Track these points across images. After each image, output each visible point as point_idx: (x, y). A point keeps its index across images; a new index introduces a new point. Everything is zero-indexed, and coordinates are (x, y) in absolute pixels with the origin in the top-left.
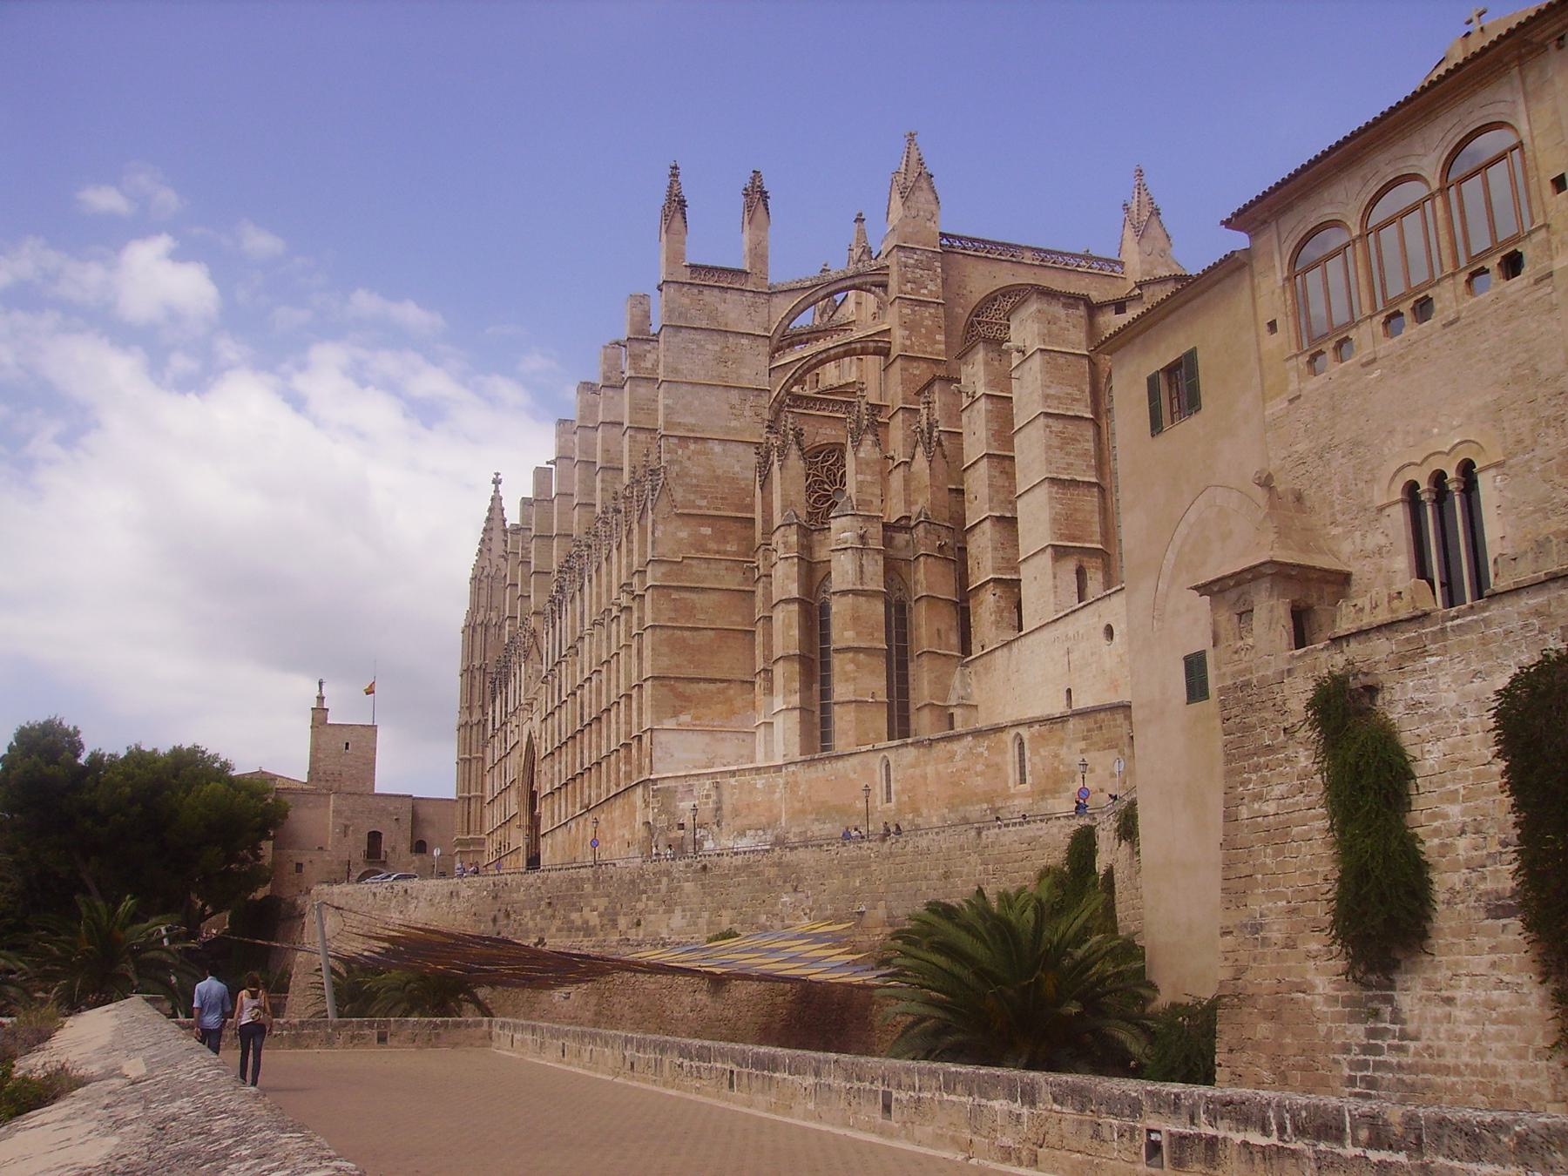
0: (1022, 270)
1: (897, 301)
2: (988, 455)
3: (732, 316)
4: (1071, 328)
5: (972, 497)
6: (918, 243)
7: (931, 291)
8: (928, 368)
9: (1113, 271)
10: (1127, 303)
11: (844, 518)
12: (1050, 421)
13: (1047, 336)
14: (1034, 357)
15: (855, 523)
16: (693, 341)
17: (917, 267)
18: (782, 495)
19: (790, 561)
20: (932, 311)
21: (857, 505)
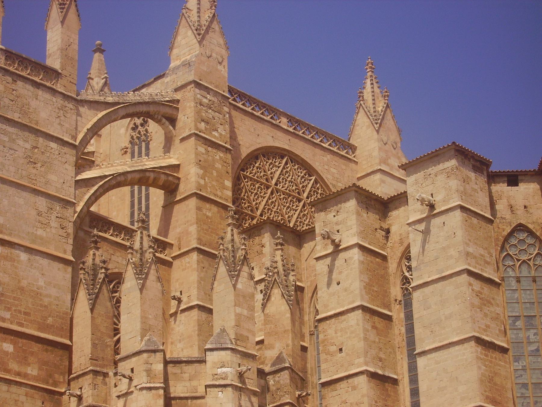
0: (279, 134)
1: (193, 139)
2: (363, 308)
3: (43, 115)
4: (479, 190)
5: (333, 349)
6: (211, 83)
7: (221, 135)
8: (218, 212)
9: (347, 153)
10: (520, 178)
11: (223, 353)
12: (472, 280)
13: (463, 194)
14: (451, 214)
15: (235, 359)
16: (5, 133)
17: (210, 108)
18: (142, 317)
19: (153, 391)
20: (222, 155)
21: (236, 339)
